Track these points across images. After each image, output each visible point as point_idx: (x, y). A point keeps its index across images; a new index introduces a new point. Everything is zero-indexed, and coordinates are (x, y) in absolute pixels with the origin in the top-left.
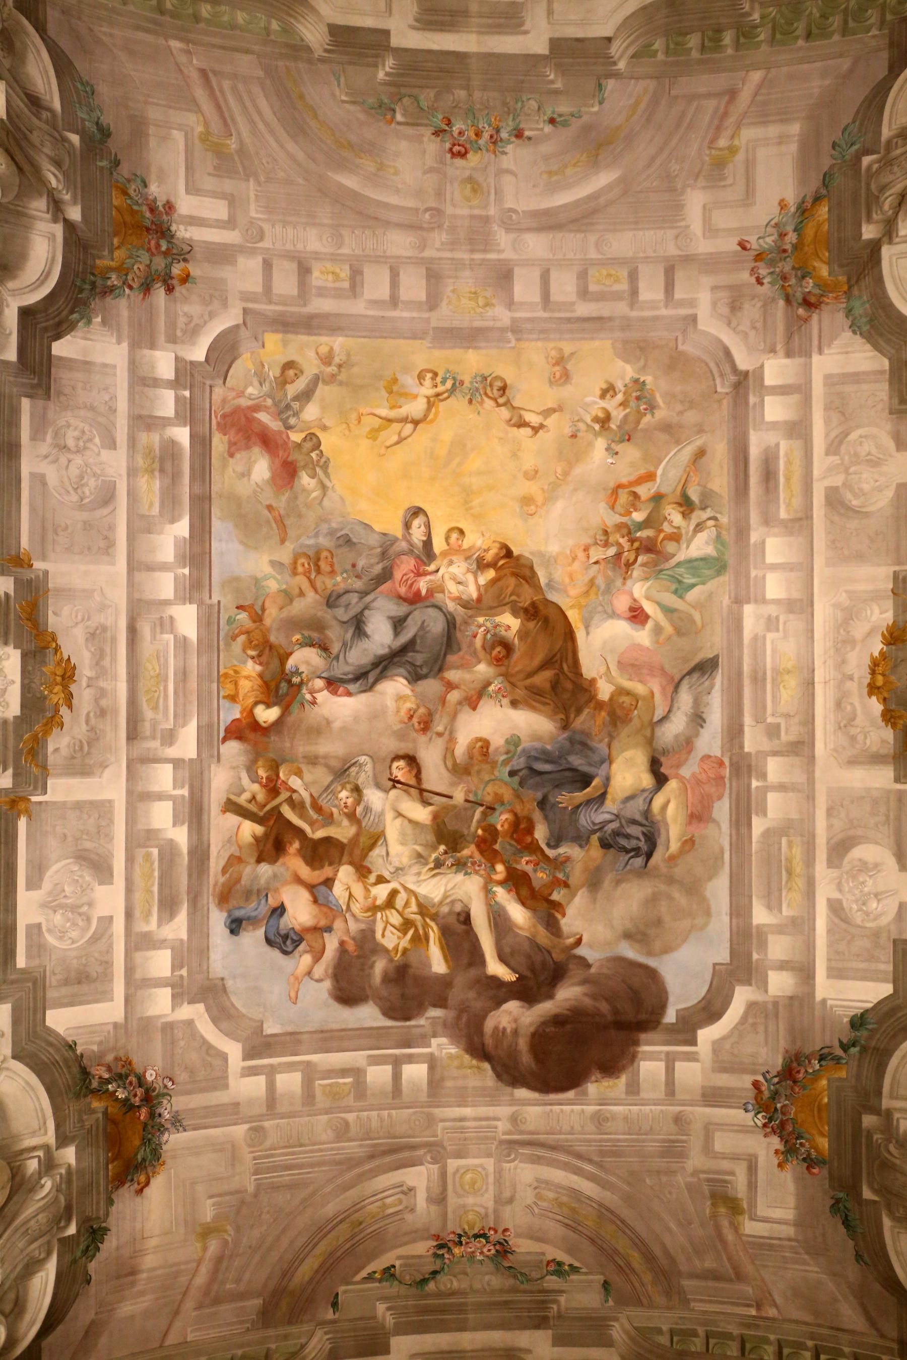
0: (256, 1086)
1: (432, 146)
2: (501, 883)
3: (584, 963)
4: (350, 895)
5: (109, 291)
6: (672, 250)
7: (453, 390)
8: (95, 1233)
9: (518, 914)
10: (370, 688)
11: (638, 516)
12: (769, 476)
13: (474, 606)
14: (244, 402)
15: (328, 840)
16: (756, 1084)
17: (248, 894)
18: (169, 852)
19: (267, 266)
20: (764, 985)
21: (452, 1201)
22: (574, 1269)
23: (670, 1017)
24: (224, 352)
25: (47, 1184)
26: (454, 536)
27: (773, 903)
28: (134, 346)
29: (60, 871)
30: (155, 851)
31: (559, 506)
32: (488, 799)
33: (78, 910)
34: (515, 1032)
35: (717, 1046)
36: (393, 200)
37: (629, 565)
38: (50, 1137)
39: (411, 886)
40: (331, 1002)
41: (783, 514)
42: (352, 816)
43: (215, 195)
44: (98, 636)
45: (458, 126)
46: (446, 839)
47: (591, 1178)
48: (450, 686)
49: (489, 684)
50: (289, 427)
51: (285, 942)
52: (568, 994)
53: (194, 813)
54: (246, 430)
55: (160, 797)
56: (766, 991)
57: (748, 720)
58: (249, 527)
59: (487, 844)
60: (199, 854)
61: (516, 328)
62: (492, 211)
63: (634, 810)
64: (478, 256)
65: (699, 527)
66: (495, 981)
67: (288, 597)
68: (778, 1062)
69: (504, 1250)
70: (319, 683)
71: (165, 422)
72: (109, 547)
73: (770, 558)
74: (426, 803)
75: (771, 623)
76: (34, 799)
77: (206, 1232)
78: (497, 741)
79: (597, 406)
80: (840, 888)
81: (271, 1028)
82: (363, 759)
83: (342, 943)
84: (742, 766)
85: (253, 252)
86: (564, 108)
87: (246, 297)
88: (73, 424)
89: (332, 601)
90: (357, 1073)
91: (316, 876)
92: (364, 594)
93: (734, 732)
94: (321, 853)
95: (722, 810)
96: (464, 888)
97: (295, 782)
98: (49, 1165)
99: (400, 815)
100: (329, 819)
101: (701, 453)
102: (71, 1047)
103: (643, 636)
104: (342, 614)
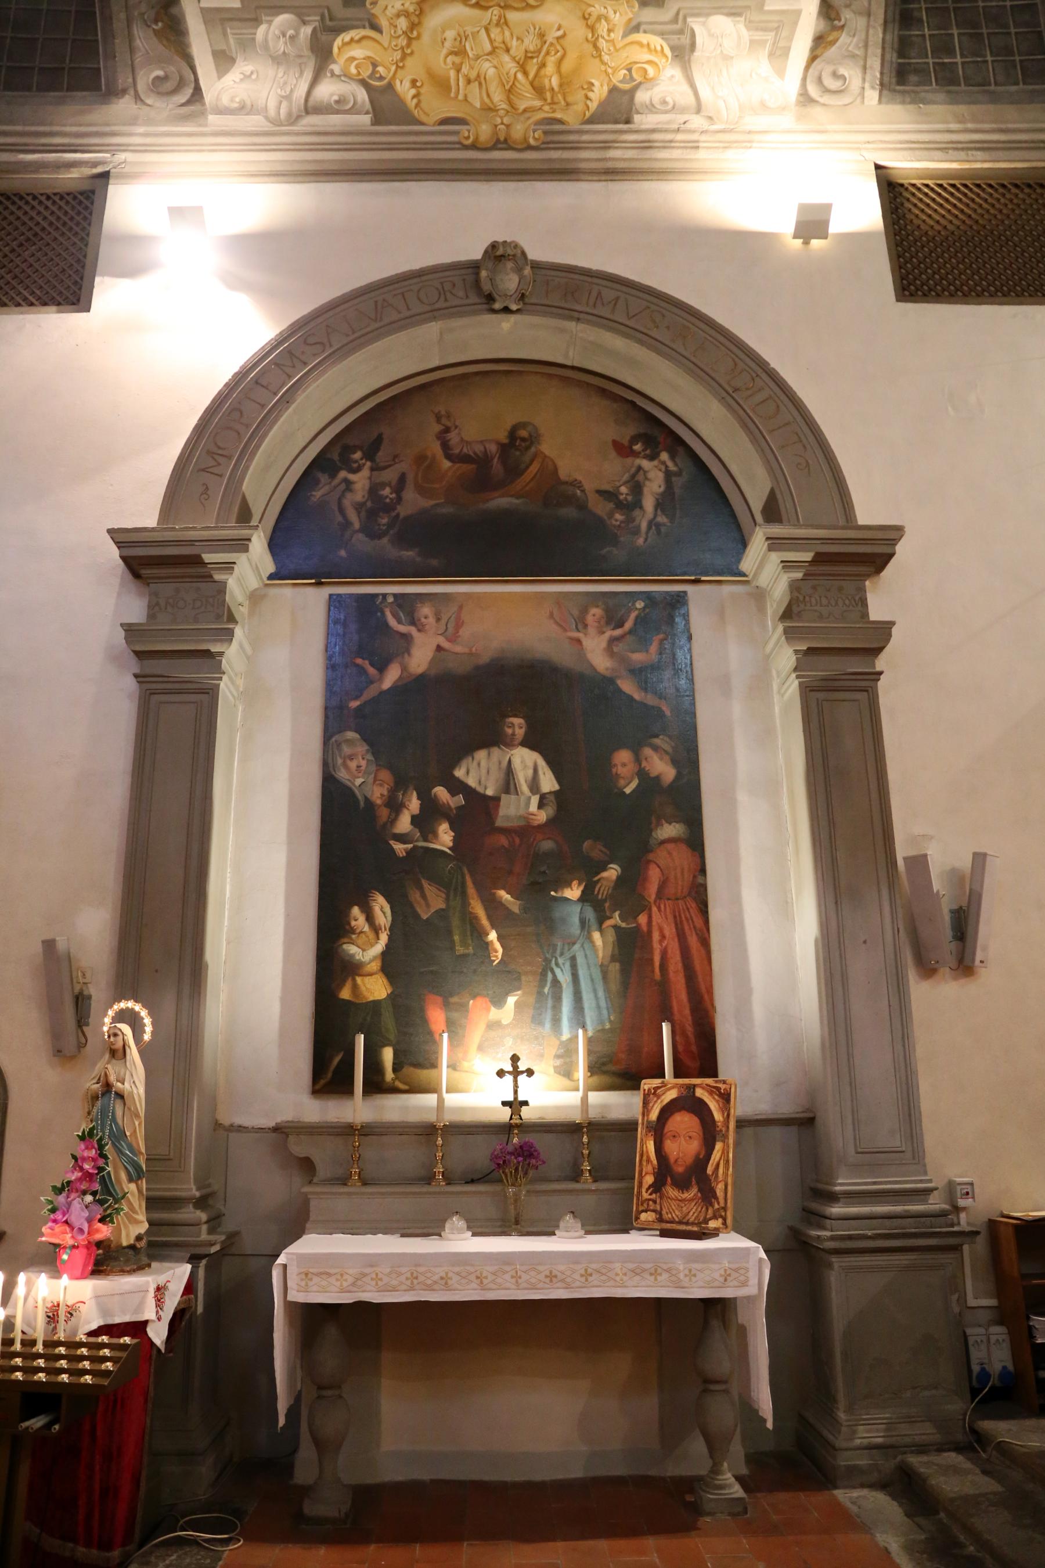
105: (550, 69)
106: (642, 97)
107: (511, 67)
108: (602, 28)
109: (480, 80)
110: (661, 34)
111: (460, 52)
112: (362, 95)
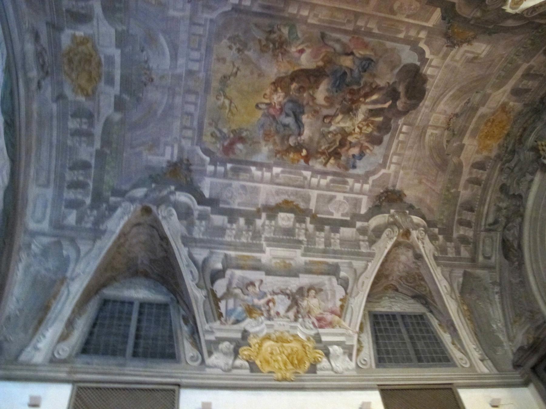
0: (393, 167)
1: (149, 87)
2: (365, 100)
3: (395, 83)
4: (356, 138)
5: (192, 180)
6: (187, 22)
7: (224, 92)
8: (411, 207)
9: (375, 97)
10: (303, 125)
11: (271, 46)
12: (268, 8)
13: (287, 94)
14: (221, 148)
15: (340, 142)
16: (447, 46)
17: (348, 163)
18: (332, 181)
19: (184, 137)
20: (420, 39)
21: (439, 124)
22: (469, 100)
23: (418, 63)
24: (207, 152)
25: (397, 217)
26: (266, 96)
27: (400, 32)
28: (205, 175)
29: (331, 208)
30: (332, 185)
31: (263, 67)
32: (341, 99)
33: (341, 204)
34: (405, 103)
35: (432, 53)
36: (165, 101)
37: (285, 50)
38: (387, 215)
39: (358, 122)
40: (381, 145)
41: (282, 6)
42: (335, 135)
43: (164, 149)
44: (278, 193)
45: (143, 78)
46: (349, 111)
47: (450, 91)
48: (308, 104)
49: (310, 94)
50: (229, 137)
51: (362, 155)
52: (401, 89)
53: (324, 174)
54: (229, 149)
55: (319, 182)
56: (423, 39)
57: (343, 27)
58: (256, 151)
59: (353, 102)
60: (334, 174)
61: (207, 71)
62: (170, 73)
63: (357, 62)
64: (183, 79)
65: (279, 30)
66: (390, 107)
67: (275, 143)
68: (444, 40)
69: (457, 115)
70: (299, 138)
71: (226, 169)
72: (255, 187)
73: (295, 12)
74: (338, 115)
75: (316, 16)
76: (314, 212)
77: (420, 182)
78: (327, 94)
79: (234, 51)
80: (403, 14)
81: (381, 161)
82: (321, 130)
83: (367, 142)
84: (356, 31)
85: (180, 141)
86: (138, 48)
87: (192, 144)
88: (226, 195)
89: (277, 132)
90: (399, 142)
91: (348, 146)
92: (277, 123)
93: (346, 32)
94: (343, 144)
95: (367, 39)
96: (363, 110)
97: (323, 148)
98: (393, 216)
99: (339, 123)
100: (335, 141)
101: (256, 25)
102: (370, 209)
103: (308, 51)
104: (282, 129)
105: (295, 359)
106: (318, 366)
107: (285, 357)
108: (307, 348)
109: (276, 361)
110: (321, 350)
111: (272, 353)
112: (247, 364)
